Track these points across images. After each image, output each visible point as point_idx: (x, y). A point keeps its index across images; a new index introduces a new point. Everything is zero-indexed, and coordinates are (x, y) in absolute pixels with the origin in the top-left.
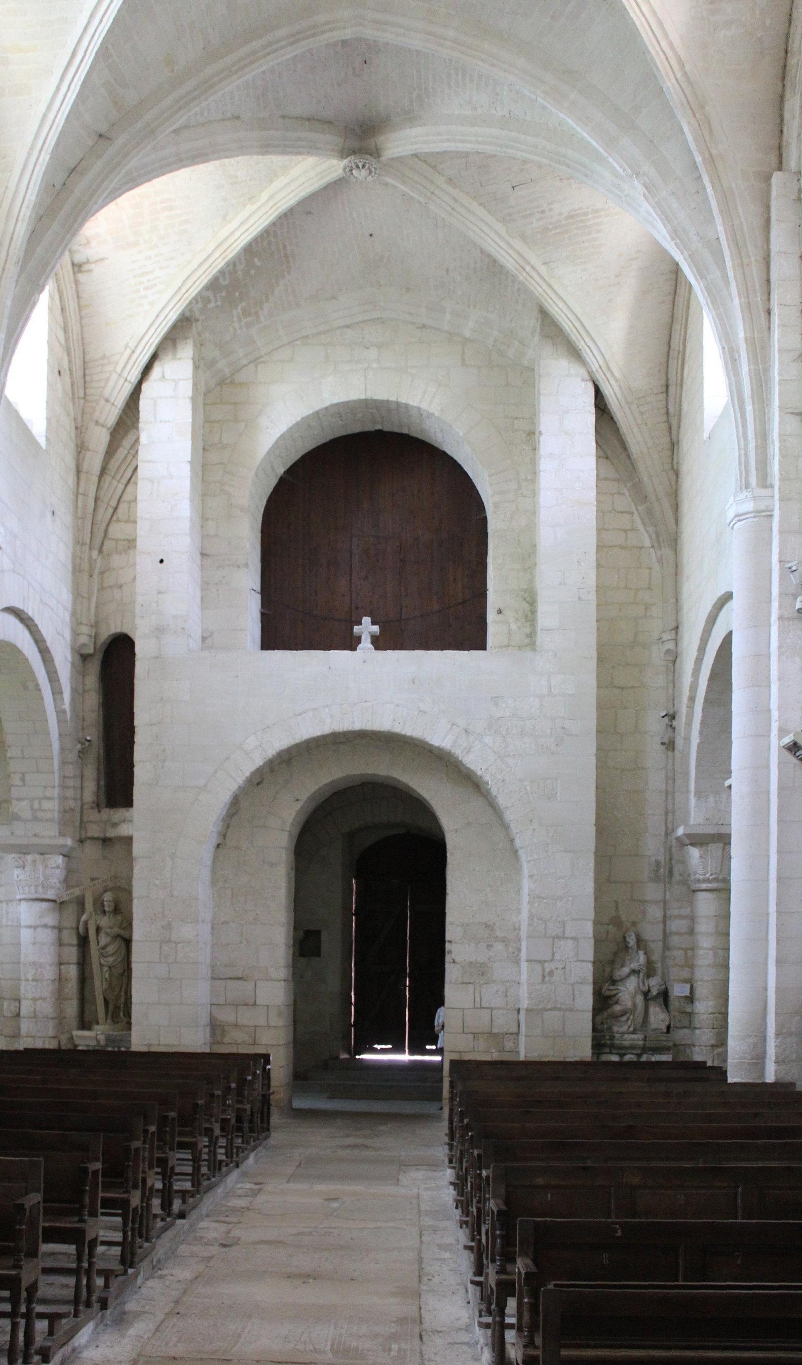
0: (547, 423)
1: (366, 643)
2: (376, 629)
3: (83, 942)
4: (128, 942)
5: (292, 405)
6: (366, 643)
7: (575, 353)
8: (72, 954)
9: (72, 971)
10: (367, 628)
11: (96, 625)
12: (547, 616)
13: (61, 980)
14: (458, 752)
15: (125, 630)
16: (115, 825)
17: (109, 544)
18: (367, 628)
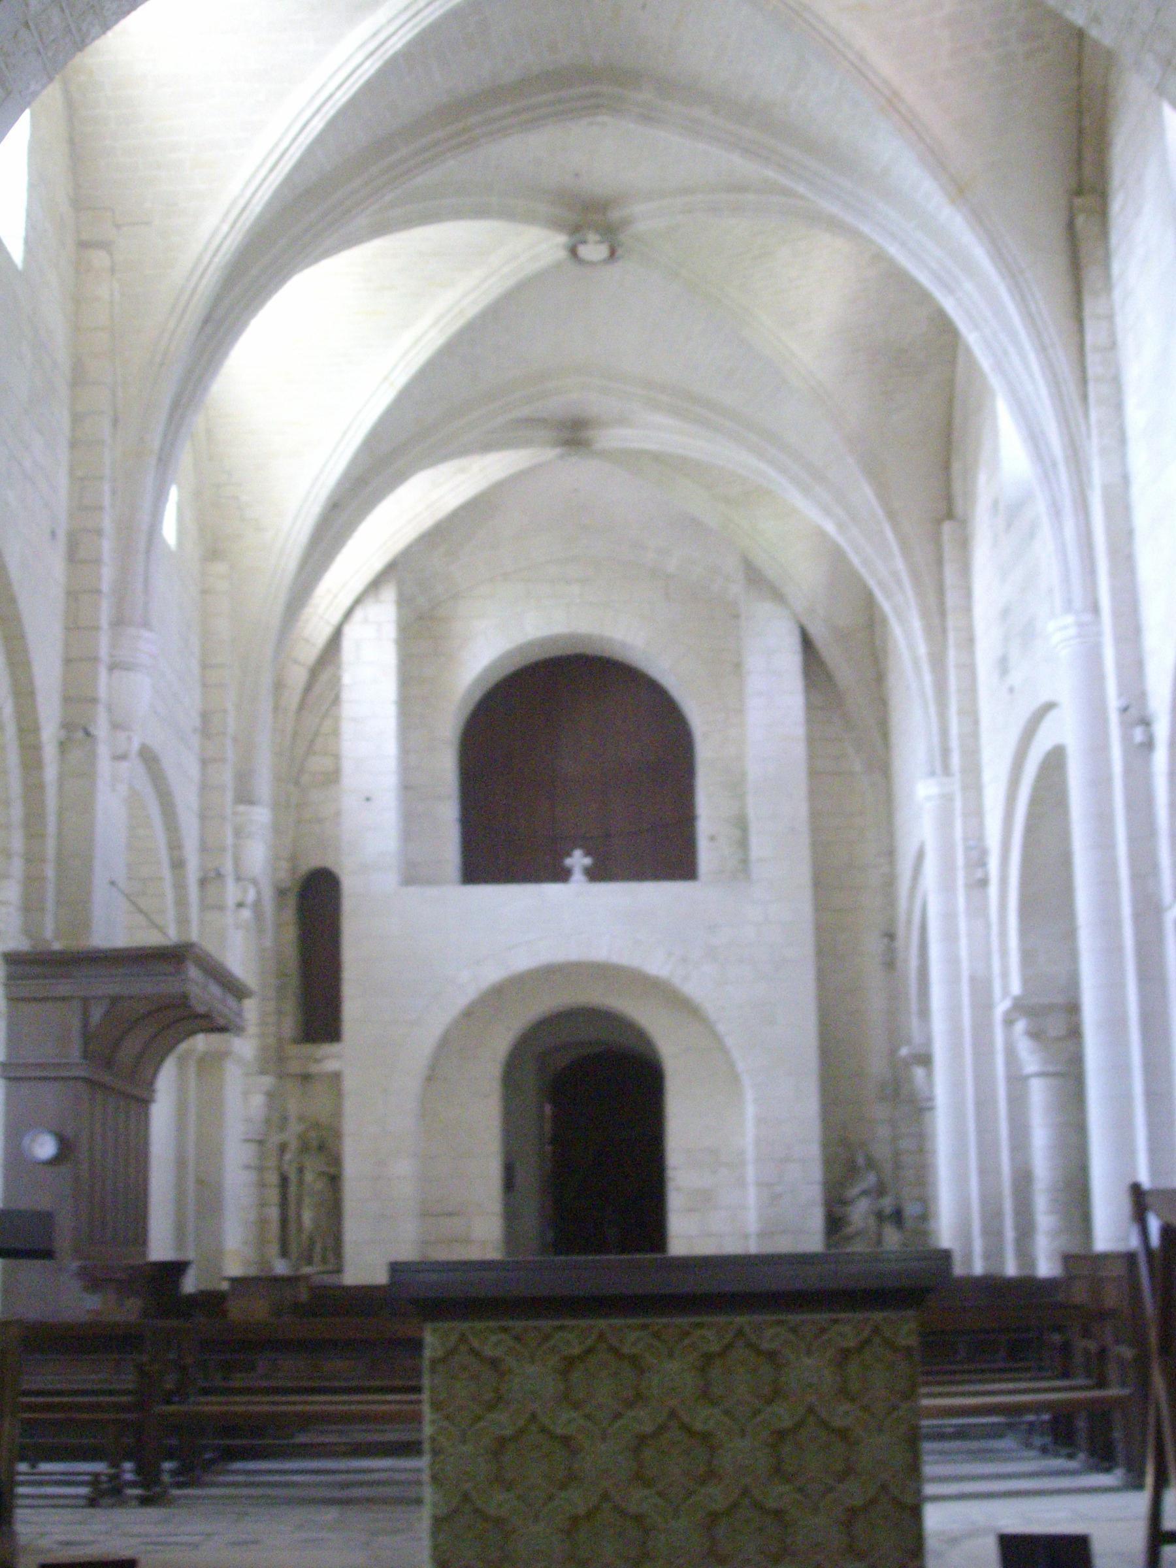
0: (754, 662)
1: (578, 876)
2: (588, 861)
3: (284, 1181)
4: (334, 1180)
5: (490, 639)
6: (578, 876)
7: (777, 595)
8: (273, 1195)
9: (274, 1213)
10: (578, 860)
11: (293, 859)
12: (759, 847)
13: (263, 1222)
14: (677, 981)
15: (329, 863)
16: (318, 1061)
17: (305, 779)
18: (578, 860)
